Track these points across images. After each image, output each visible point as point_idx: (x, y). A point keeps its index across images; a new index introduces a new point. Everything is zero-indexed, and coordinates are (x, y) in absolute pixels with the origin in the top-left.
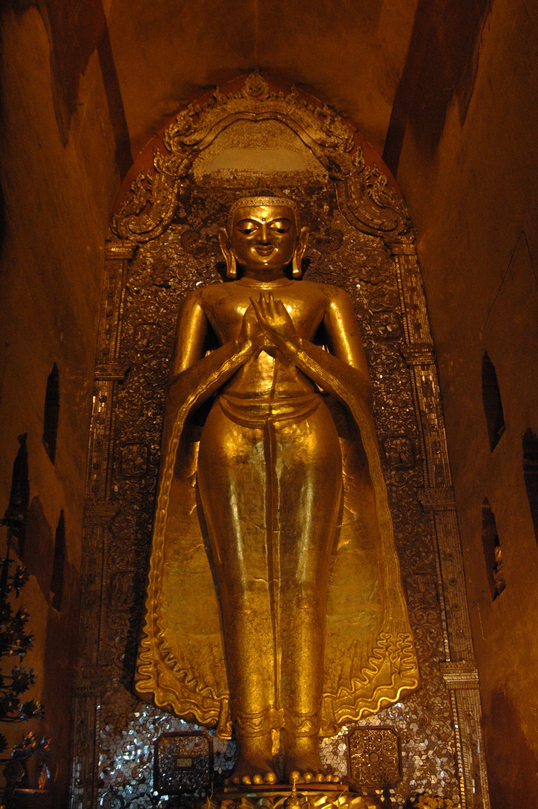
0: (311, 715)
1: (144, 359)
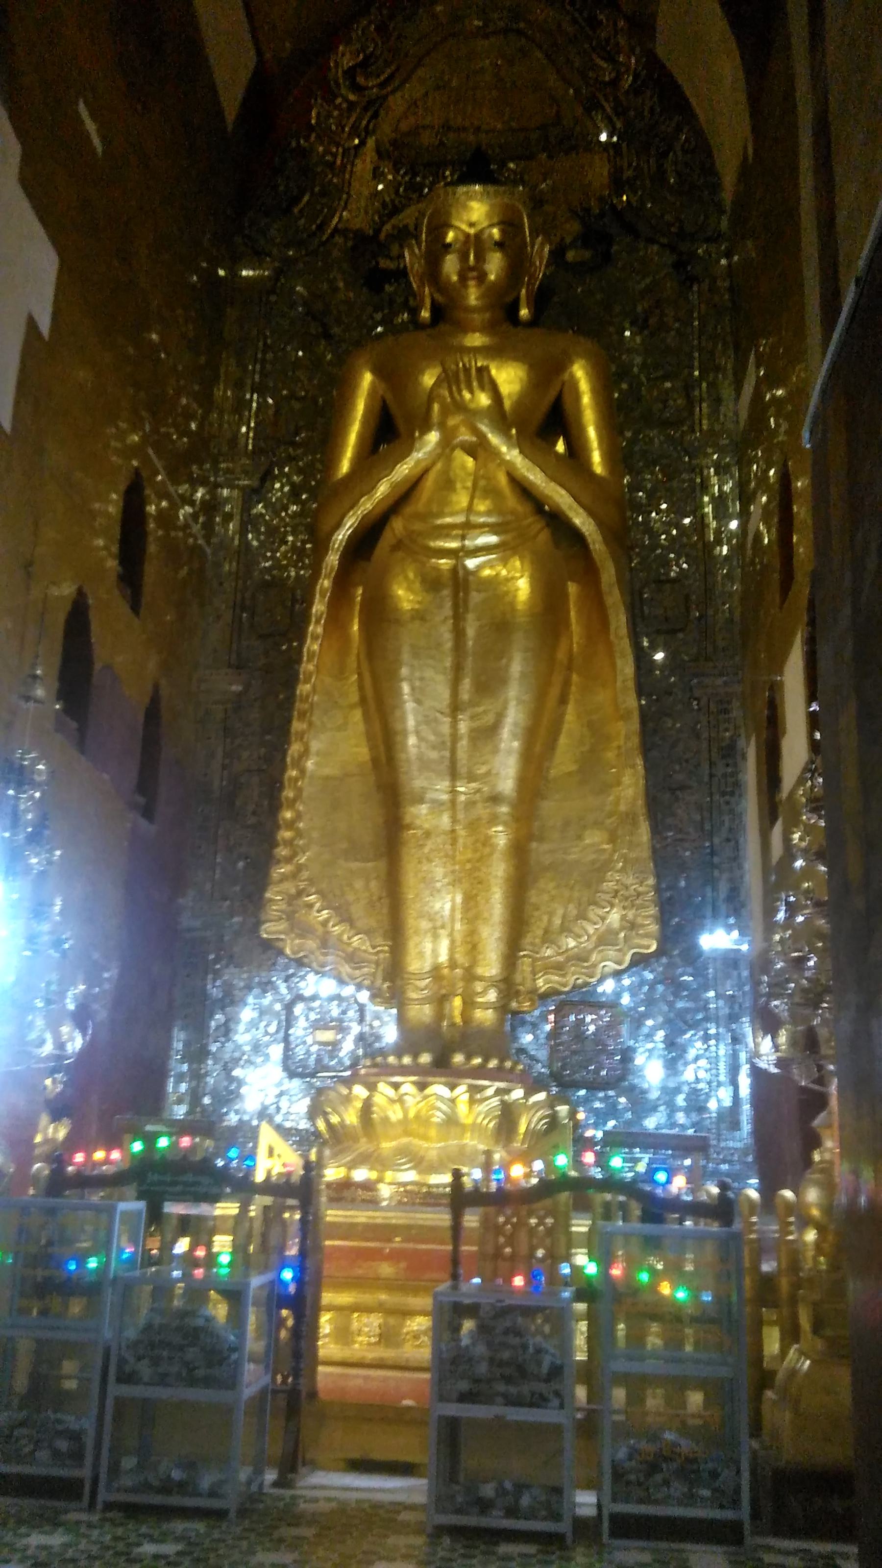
0: (498, 978)
1: (290, 455)
